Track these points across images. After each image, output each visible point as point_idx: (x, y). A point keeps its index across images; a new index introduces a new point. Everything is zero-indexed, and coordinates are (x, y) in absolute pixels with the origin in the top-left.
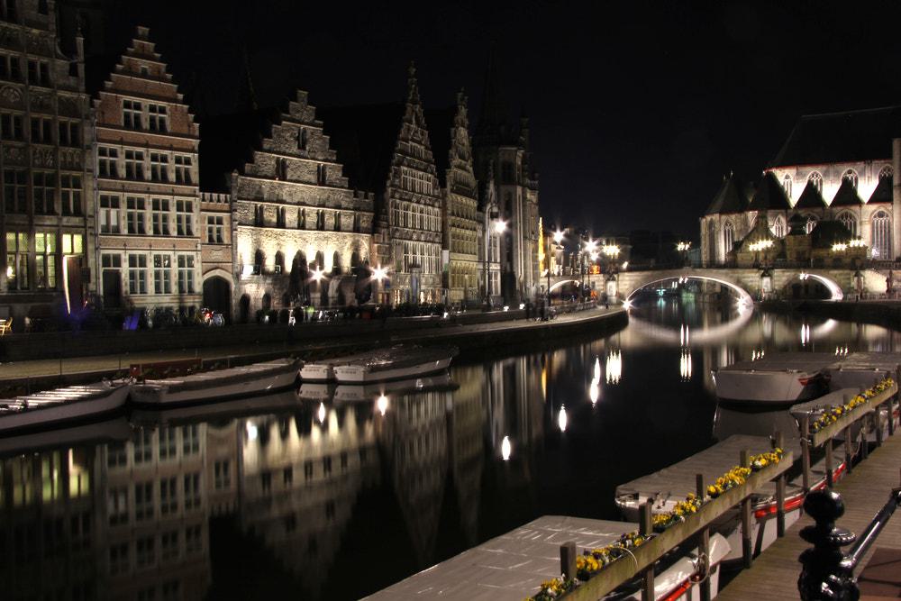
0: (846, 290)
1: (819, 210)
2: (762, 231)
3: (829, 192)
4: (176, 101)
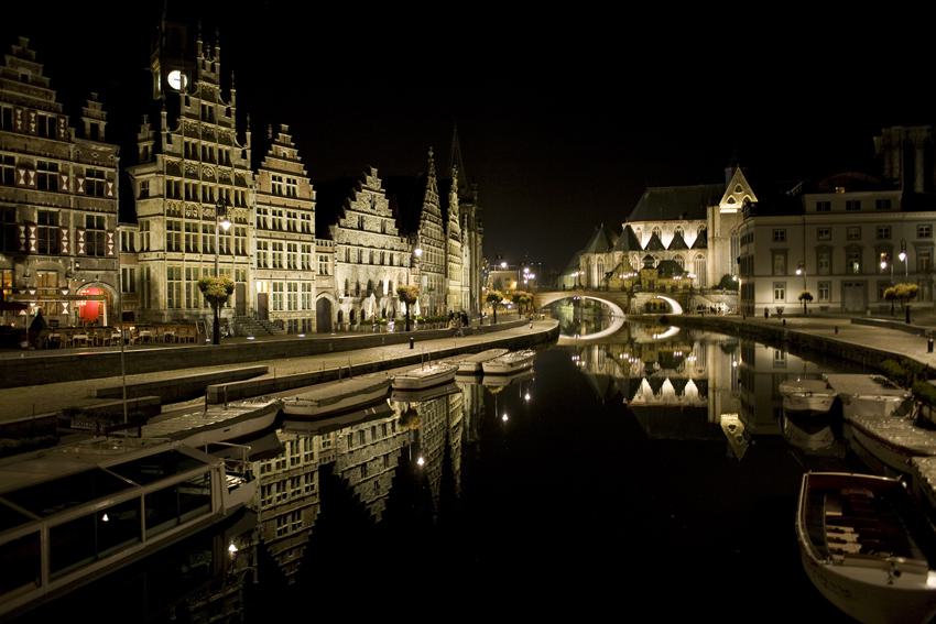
3: (667, 240)
4: (303, 175)
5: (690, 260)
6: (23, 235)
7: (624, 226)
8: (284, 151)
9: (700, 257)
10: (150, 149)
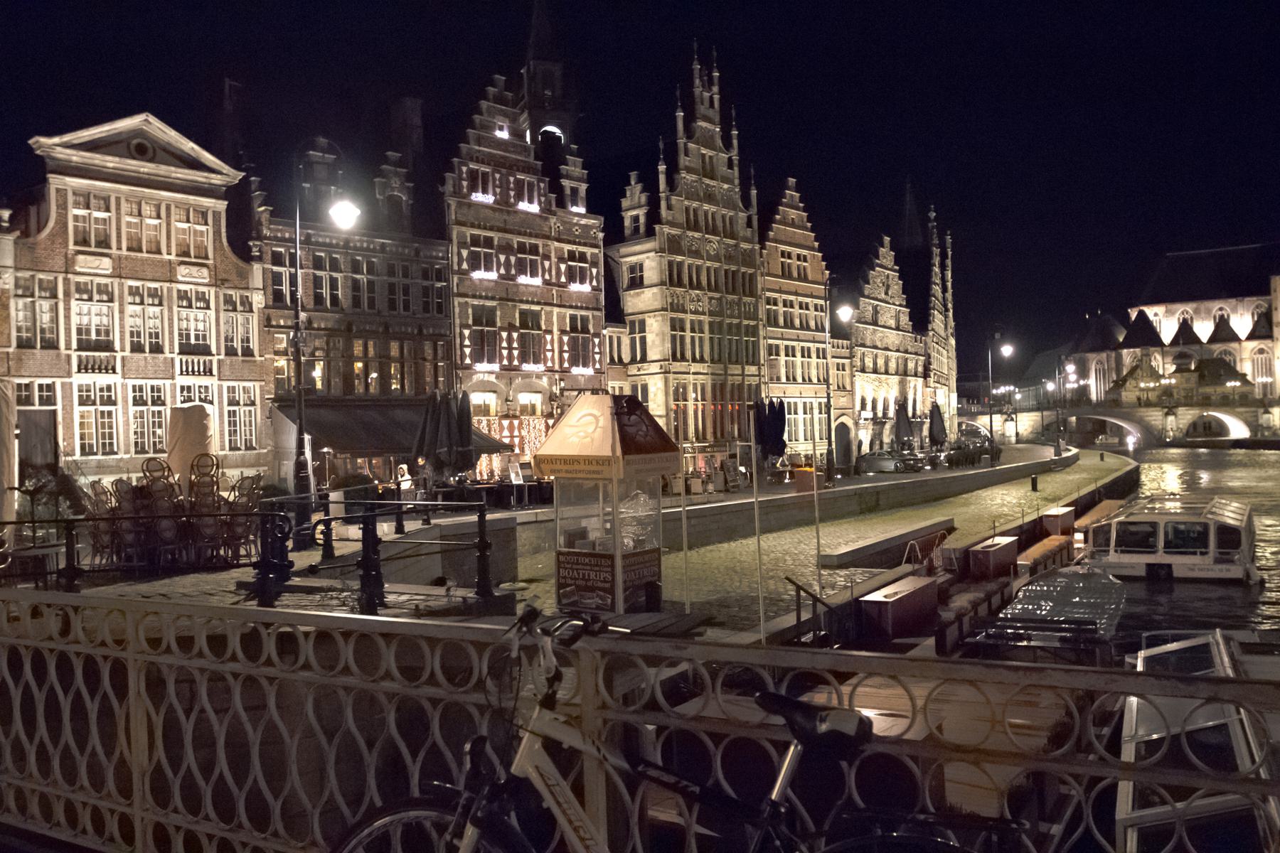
0: (1254, 426)
1: (1197, 347)
3: (1204, 329)
6: (505, 344)
7: (1134, 314)
8: (792, 211)
9: (1261, 351)
10: (642, 220)
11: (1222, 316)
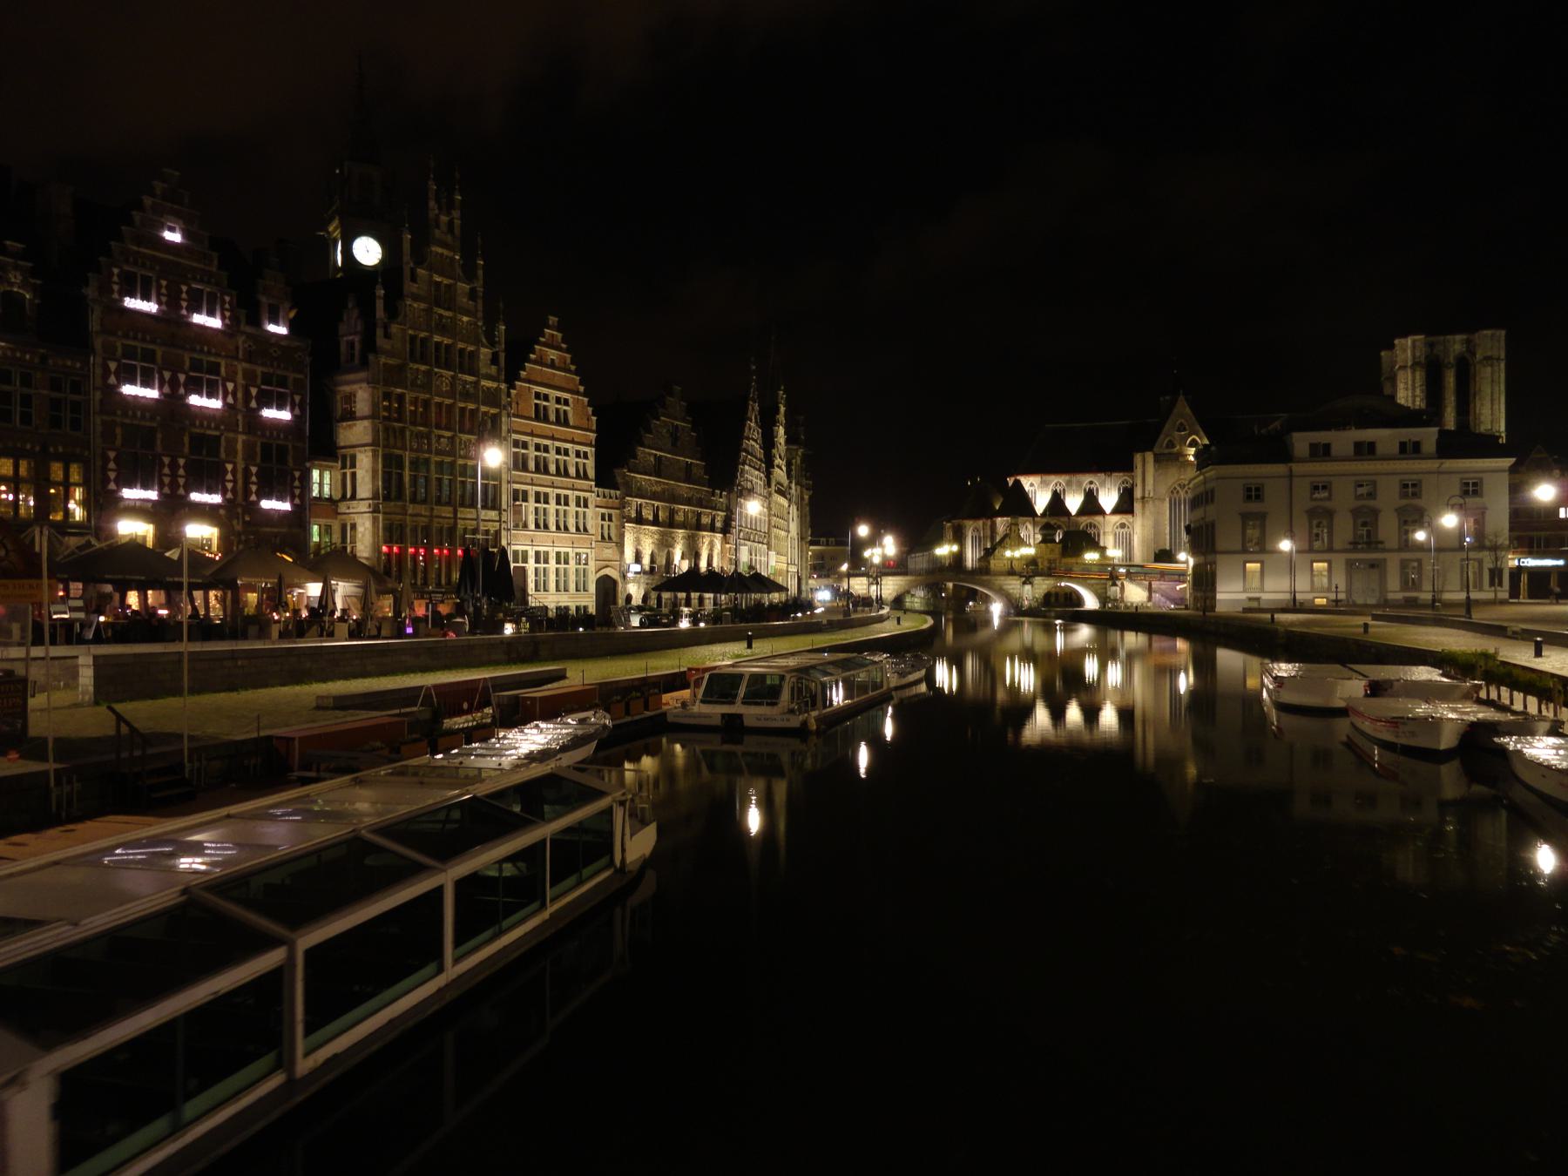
0: (1103, 598)
1: (1065, 519)
2: (1013, 538)
3: (1073, 502)
4: (578, 393)
5: (1109, 528)
7: (1011, 481)
8: (551, 351)
10: (357, 346)
11: (1091, 491)
